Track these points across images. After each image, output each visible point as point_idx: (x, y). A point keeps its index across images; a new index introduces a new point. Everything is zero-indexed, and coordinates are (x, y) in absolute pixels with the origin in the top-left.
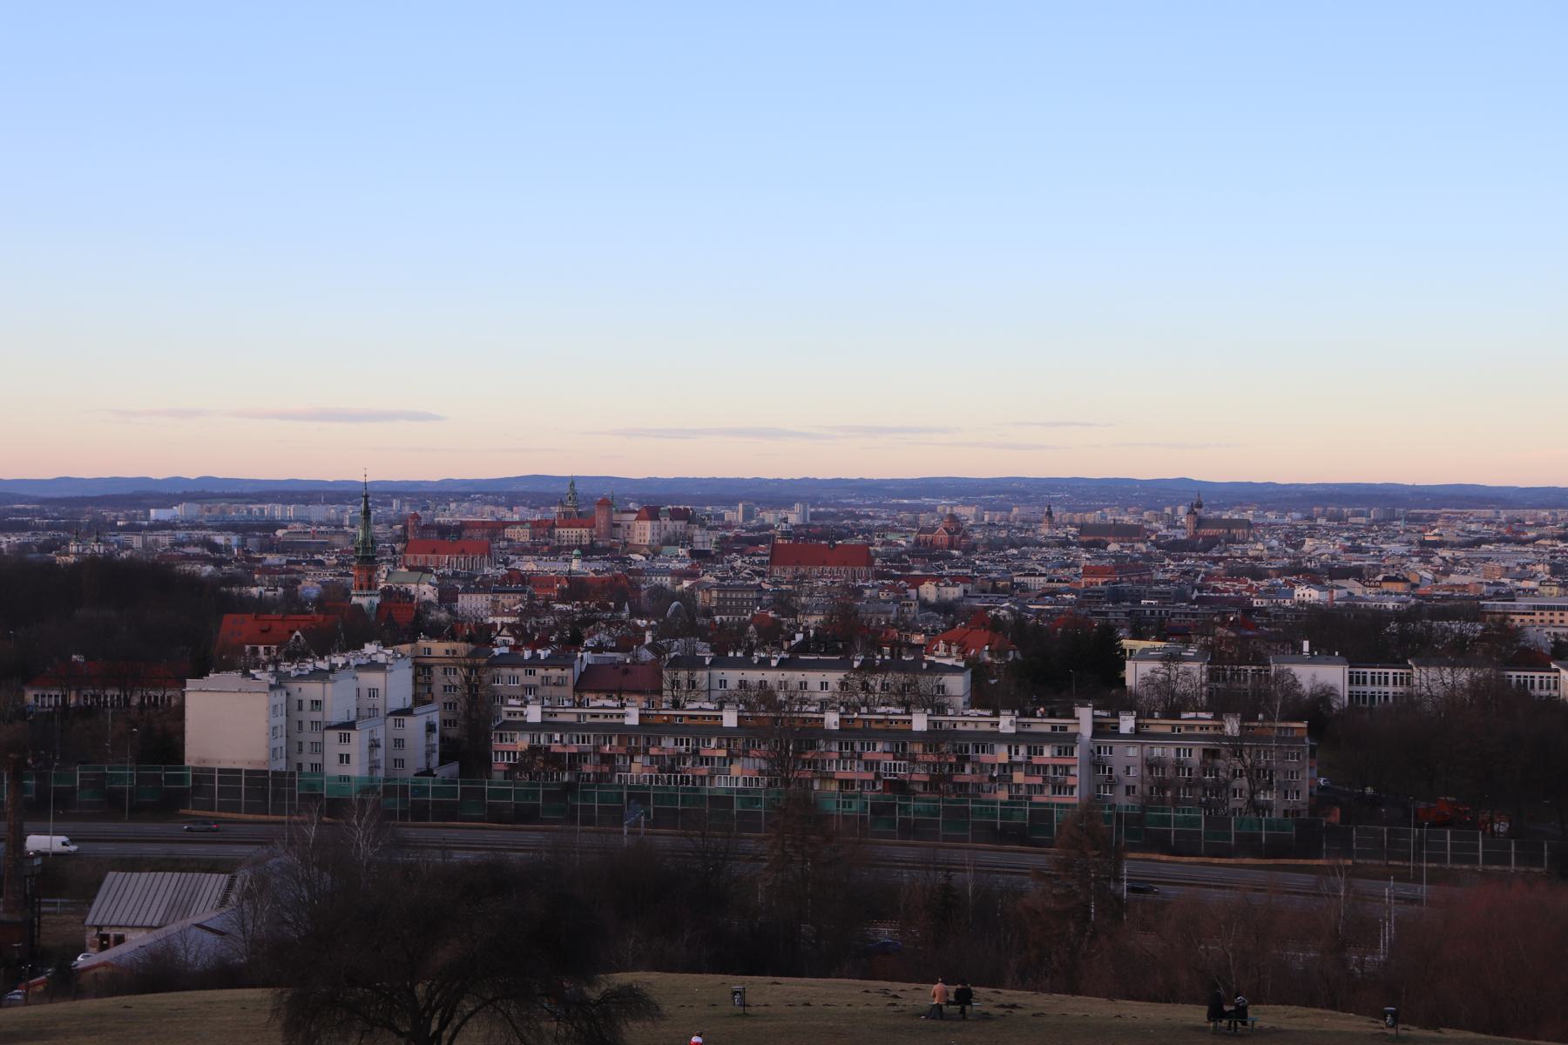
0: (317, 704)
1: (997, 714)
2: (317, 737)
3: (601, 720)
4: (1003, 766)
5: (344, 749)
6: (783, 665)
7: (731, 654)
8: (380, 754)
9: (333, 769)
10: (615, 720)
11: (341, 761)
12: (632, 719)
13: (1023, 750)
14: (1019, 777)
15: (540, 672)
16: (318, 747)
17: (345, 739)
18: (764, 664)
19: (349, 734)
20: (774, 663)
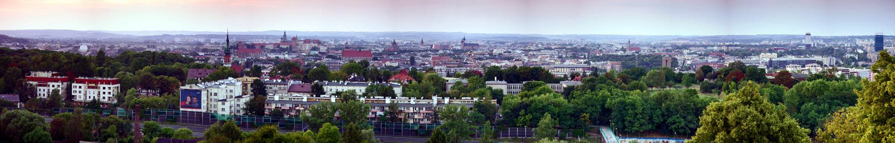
0: (216, 94)
1: (410, 99)
2: (215, 103)
3: (296, 100)
4: (412, 113)
5: (223, 107)
6: (348, 84)
7: (333, 81)
8: (233, 108)
9: (220, 113)
10: (300, 100)
12: (305, 100)
13: (417, 109)
14: (416, 116)
15: (278, 86)
16: (215, 106)
17: (223, 104)
18: (343, 85)
20: (346, 84)
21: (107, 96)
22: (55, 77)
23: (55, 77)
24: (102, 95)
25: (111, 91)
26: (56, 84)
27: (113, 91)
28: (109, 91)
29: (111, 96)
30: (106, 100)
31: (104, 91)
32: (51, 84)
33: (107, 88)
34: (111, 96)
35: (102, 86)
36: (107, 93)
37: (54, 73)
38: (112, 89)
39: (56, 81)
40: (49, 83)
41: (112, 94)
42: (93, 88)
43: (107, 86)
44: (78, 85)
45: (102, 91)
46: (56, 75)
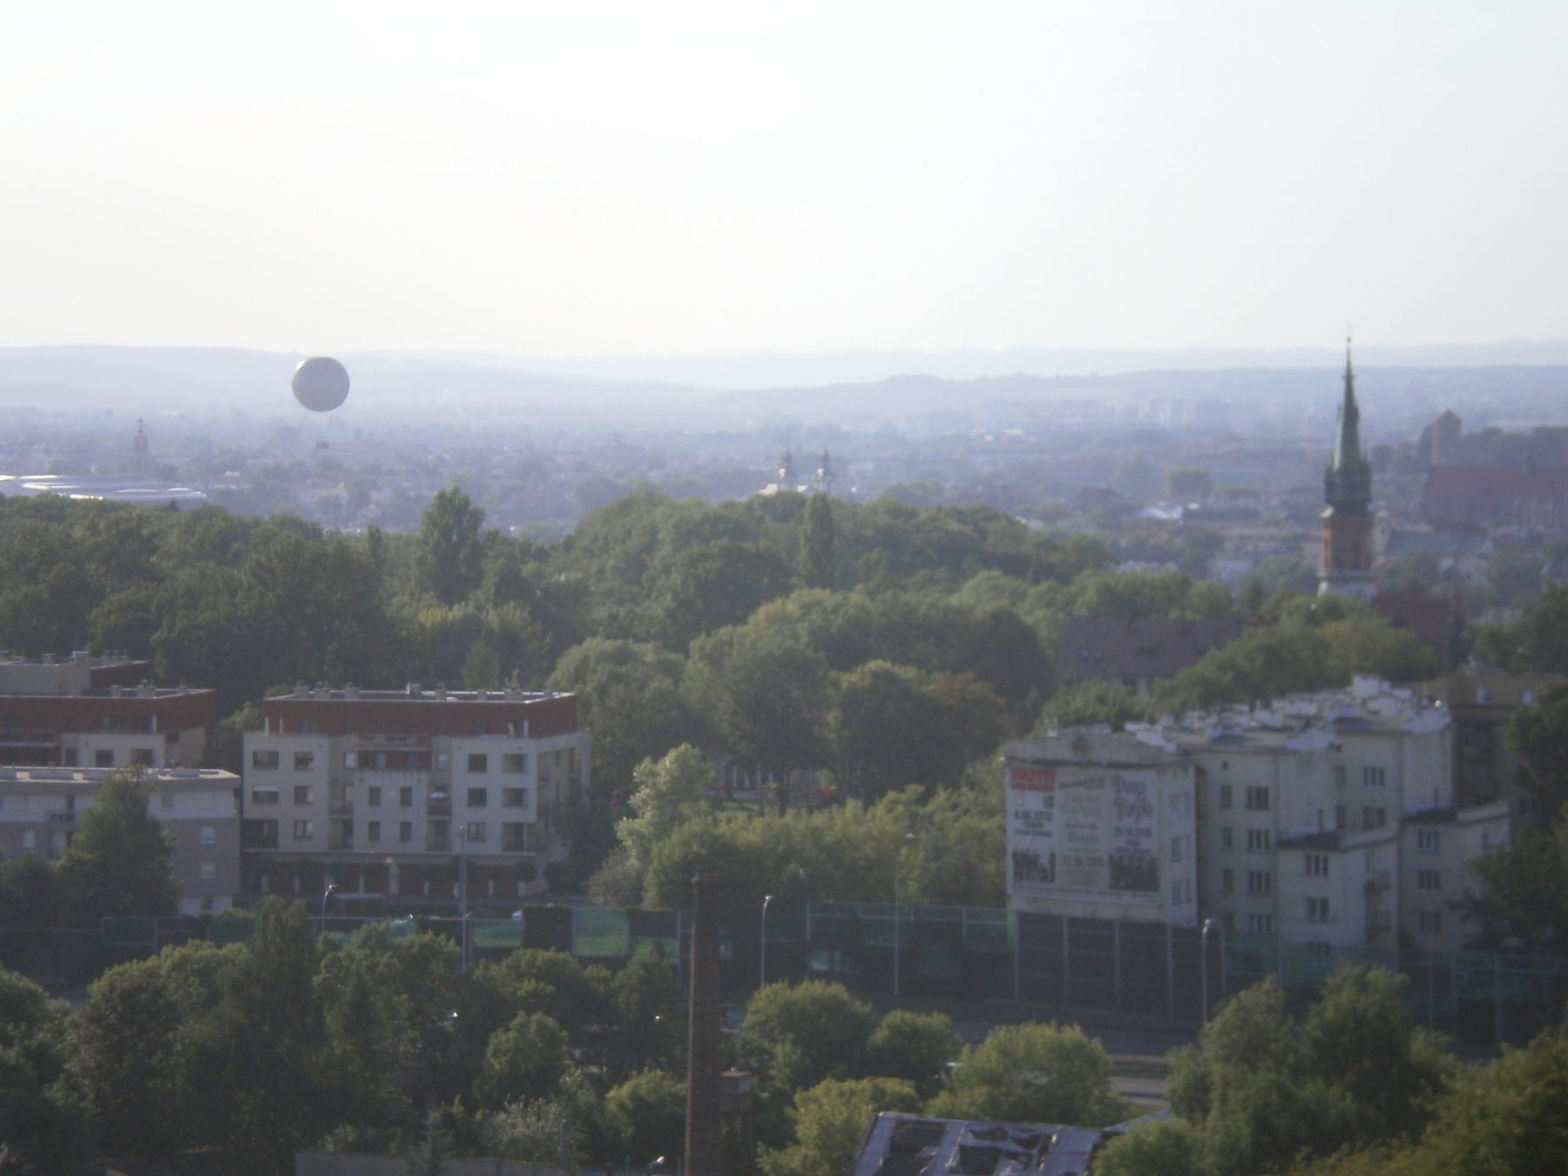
0: (1259, 798)
2: (1259, 862)
11: (1312, 911)
16: (1261, 883)
19: (1326, 860)
21: (496, 815)
22: (116, 693)
23: (116, 693)
24: (462, 816)
25: (528, 781)
26: (124, 744)
27: (543, 779)
28: (515, 781)
29: (528, 815)
30: (493, 846)
31: (477, 780)
32: (88, 743)
33: (495, 763)
34: (528, 815)
35: (457, 751)
36: (495, 797)
37: (109, 663)
38: (532, 765)
39: (134, 719)
40: (69, 740)
41: (532, 798)
42: (398, 762)
43: (495, 747)
44: (288, 746)
45: (462, 781)
46: (127, 677)
